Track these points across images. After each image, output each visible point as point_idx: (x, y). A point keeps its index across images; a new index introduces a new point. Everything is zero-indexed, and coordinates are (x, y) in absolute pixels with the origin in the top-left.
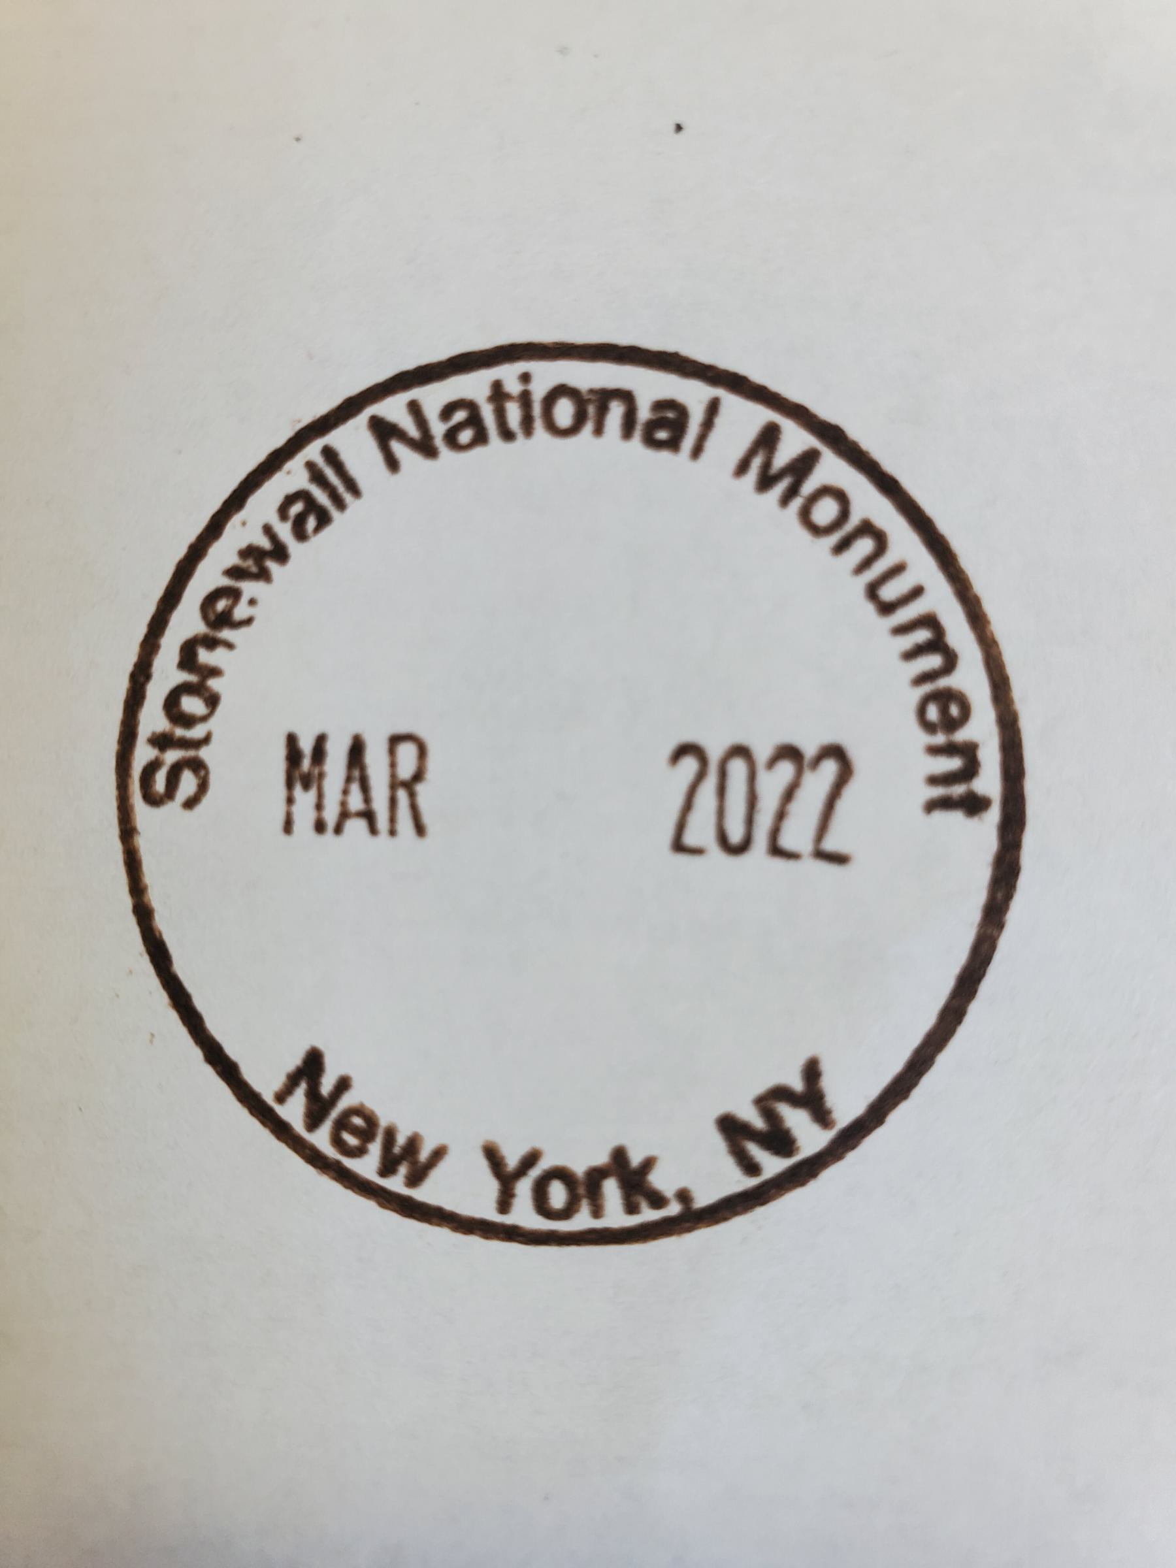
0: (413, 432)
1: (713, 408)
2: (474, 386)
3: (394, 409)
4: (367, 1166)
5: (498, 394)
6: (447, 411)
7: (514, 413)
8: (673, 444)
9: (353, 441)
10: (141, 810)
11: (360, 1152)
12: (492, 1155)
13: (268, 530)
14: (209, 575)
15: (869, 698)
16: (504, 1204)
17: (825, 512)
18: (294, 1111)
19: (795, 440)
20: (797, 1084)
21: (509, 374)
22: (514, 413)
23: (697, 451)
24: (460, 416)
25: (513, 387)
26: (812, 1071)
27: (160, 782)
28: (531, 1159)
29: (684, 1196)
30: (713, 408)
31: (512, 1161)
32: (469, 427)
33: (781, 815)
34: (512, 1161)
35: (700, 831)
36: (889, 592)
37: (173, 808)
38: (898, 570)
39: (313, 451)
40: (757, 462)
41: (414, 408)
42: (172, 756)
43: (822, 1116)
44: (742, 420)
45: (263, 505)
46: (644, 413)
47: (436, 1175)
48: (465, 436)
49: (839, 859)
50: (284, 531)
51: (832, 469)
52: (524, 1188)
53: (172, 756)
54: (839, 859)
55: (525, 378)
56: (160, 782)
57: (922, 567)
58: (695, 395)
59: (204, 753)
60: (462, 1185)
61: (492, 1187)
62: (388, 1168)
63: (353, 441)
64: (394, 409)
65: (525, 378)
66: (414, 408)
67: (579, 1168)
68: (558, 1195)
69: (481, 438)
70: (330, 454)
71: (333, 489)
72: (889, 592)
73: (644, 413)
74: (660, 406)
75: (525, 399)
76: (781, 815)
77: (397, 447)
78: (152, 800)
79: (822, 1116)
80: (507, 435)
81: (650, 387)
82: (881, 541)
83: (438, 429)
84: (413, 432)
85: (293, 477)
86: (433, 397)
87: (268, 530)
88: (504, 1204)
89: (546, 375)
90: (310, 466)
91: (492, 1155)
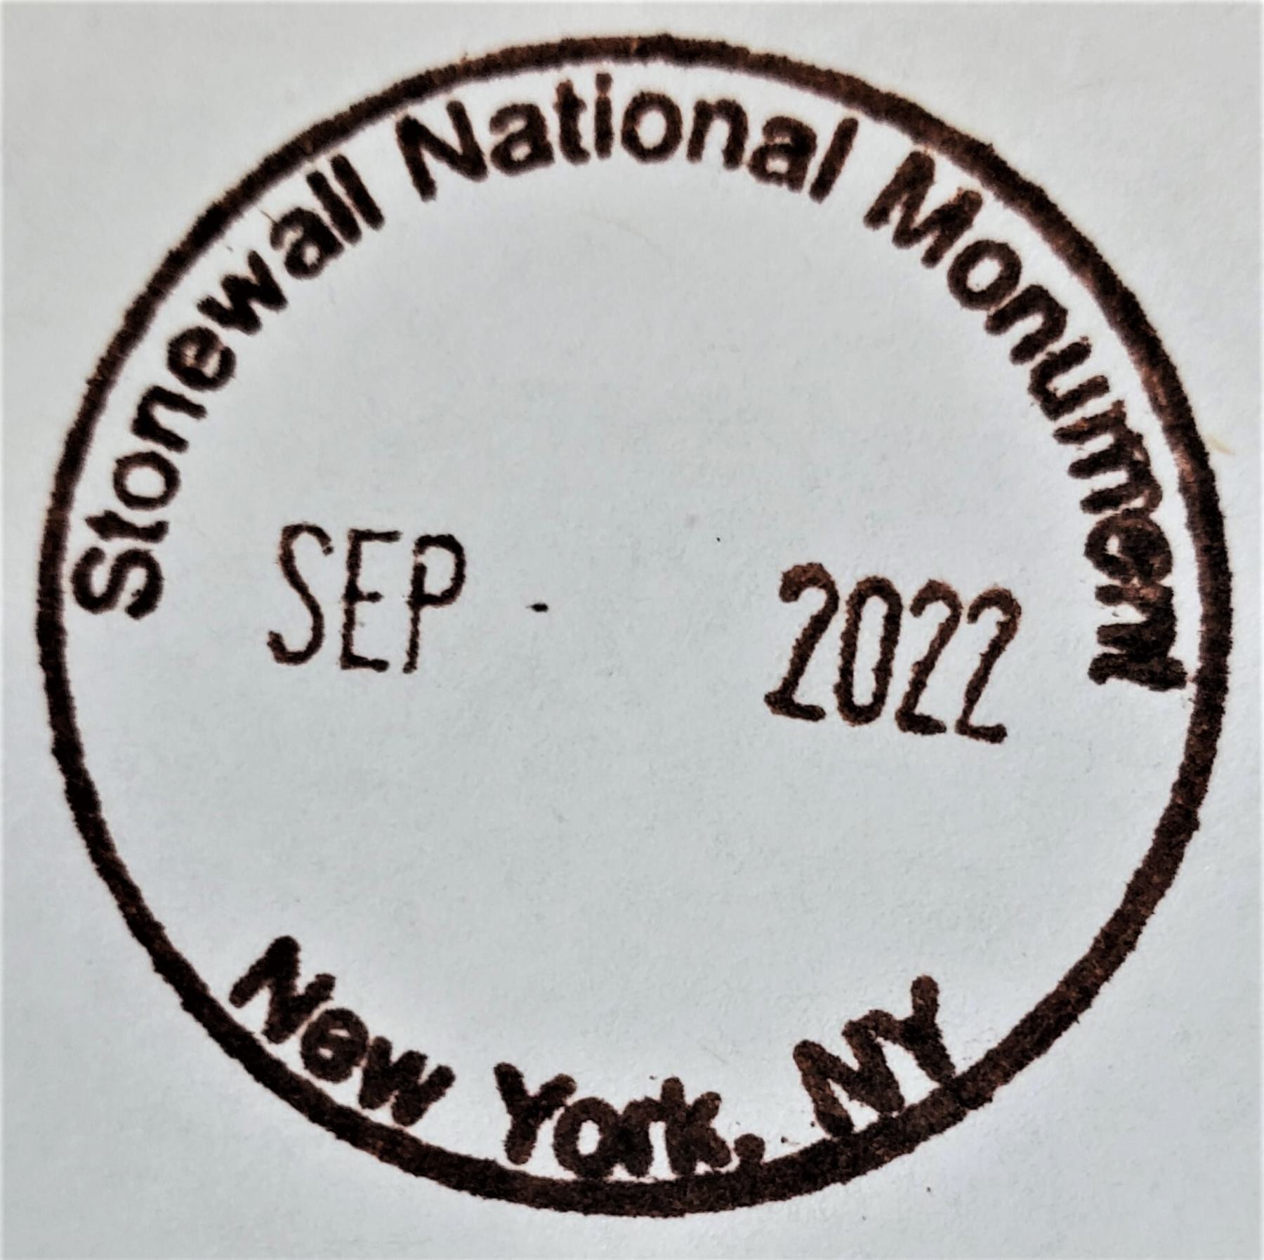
0: (451, 138)
1: (846, 133)
2: (537, 87)
3: (432, 114)
4: (345, 1093)
5: (569, 104)
6: (499, 121)
7: (586, 124)
8: (793, 179)
9: (375, 153)
10: (72, 614)
11: (336, 1072)
12: (508, 1079)
13: (255, 261)
14: (178, 313)
15: (1029, 522)
16: (520, 1142)
17: (985, 273)
18: (253, 1016)
19: (950, 180)
20: (902, 1009)
21: (582, 78)
22: (586, 124)
23: (822, 188)
24: (517, 125)
25: (586, 90)
26: (925, 991)
27: (99, 579)
28: (560, 1087)
29: (751, 1146)
30: (846, 133)
31: (533, 1087)
32: (526, 143)
33: (924, 668)
34: (533, 1087)
35: (818, 685)
36: (1063, 384)
37: (117, 615)
38: (1079, 352)
39: (323, 164)
40: (896, 215)
41: (458, 114)
42: (115, 547)
43: (932, 1055)
44: (881, 150)
45: (250, 232)
46: (755, 139)
47: (436, 1110)
48: (521, 152)
49: (996, 734)
50: (275, 261)
51: (997, 220)
52: (546, 1132)
53: (115, 547)
54: (996, 734)
55: (604, 81)
56: (99, 579)
57: (1111, 357)
58: (822, 115)
59: (157, 550)
60: (467, 1122)
61: (503, 1122)
62: (369, 1097)
63: (375, 153)
64: (432, 114)
65: (604, 81)
66: (458, 114)
67: (619, 1104)
68: (589, 1139)
69: (541, 154)
70: (343, 168)
71: (345, 214)
72: (1063, 384)
73: (755, 139)
74: (776, 125)
75: (603, 109)
76: (924, 668)
77: (429, 159)
78: (92, 603)
79: (932, 1055)
80: (575, 152)
81: (764, 99)
82: (1056, 317)
83: (486, 140)
84: (451, 138)
85: (292, 192)
86: (482, 99)
87: (255, 261)
88: (520, 1142)
89: (630, 80)
90: (317, 181)
91: (508, 1079)
